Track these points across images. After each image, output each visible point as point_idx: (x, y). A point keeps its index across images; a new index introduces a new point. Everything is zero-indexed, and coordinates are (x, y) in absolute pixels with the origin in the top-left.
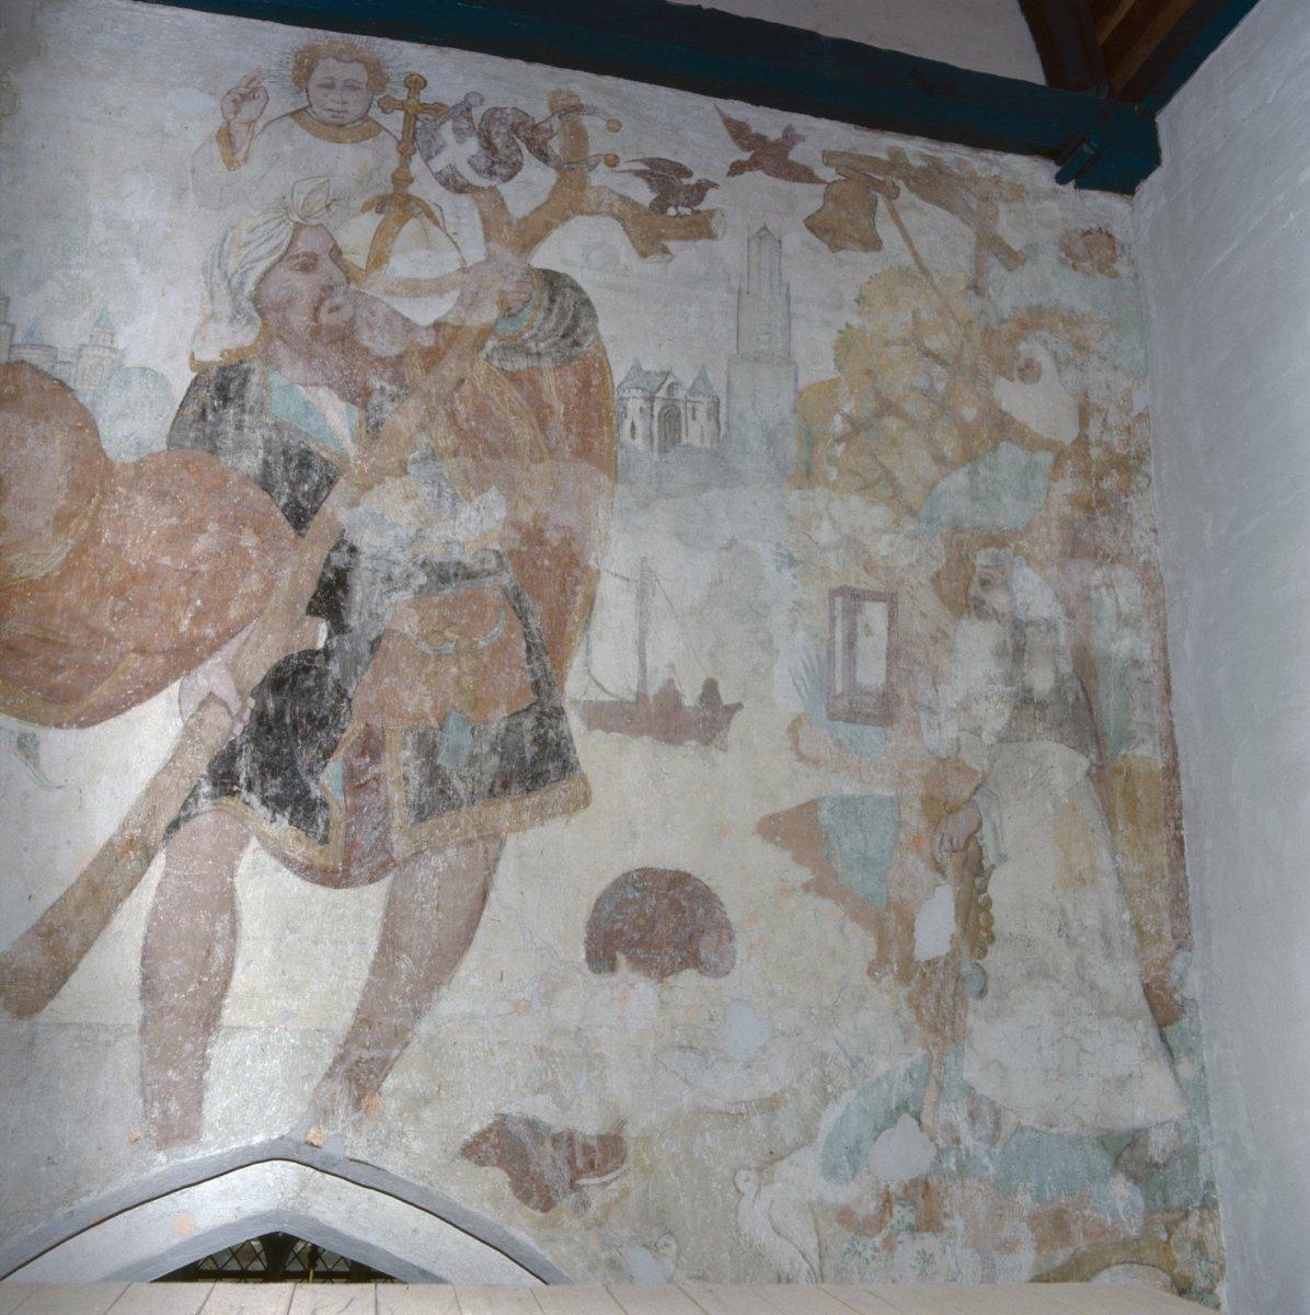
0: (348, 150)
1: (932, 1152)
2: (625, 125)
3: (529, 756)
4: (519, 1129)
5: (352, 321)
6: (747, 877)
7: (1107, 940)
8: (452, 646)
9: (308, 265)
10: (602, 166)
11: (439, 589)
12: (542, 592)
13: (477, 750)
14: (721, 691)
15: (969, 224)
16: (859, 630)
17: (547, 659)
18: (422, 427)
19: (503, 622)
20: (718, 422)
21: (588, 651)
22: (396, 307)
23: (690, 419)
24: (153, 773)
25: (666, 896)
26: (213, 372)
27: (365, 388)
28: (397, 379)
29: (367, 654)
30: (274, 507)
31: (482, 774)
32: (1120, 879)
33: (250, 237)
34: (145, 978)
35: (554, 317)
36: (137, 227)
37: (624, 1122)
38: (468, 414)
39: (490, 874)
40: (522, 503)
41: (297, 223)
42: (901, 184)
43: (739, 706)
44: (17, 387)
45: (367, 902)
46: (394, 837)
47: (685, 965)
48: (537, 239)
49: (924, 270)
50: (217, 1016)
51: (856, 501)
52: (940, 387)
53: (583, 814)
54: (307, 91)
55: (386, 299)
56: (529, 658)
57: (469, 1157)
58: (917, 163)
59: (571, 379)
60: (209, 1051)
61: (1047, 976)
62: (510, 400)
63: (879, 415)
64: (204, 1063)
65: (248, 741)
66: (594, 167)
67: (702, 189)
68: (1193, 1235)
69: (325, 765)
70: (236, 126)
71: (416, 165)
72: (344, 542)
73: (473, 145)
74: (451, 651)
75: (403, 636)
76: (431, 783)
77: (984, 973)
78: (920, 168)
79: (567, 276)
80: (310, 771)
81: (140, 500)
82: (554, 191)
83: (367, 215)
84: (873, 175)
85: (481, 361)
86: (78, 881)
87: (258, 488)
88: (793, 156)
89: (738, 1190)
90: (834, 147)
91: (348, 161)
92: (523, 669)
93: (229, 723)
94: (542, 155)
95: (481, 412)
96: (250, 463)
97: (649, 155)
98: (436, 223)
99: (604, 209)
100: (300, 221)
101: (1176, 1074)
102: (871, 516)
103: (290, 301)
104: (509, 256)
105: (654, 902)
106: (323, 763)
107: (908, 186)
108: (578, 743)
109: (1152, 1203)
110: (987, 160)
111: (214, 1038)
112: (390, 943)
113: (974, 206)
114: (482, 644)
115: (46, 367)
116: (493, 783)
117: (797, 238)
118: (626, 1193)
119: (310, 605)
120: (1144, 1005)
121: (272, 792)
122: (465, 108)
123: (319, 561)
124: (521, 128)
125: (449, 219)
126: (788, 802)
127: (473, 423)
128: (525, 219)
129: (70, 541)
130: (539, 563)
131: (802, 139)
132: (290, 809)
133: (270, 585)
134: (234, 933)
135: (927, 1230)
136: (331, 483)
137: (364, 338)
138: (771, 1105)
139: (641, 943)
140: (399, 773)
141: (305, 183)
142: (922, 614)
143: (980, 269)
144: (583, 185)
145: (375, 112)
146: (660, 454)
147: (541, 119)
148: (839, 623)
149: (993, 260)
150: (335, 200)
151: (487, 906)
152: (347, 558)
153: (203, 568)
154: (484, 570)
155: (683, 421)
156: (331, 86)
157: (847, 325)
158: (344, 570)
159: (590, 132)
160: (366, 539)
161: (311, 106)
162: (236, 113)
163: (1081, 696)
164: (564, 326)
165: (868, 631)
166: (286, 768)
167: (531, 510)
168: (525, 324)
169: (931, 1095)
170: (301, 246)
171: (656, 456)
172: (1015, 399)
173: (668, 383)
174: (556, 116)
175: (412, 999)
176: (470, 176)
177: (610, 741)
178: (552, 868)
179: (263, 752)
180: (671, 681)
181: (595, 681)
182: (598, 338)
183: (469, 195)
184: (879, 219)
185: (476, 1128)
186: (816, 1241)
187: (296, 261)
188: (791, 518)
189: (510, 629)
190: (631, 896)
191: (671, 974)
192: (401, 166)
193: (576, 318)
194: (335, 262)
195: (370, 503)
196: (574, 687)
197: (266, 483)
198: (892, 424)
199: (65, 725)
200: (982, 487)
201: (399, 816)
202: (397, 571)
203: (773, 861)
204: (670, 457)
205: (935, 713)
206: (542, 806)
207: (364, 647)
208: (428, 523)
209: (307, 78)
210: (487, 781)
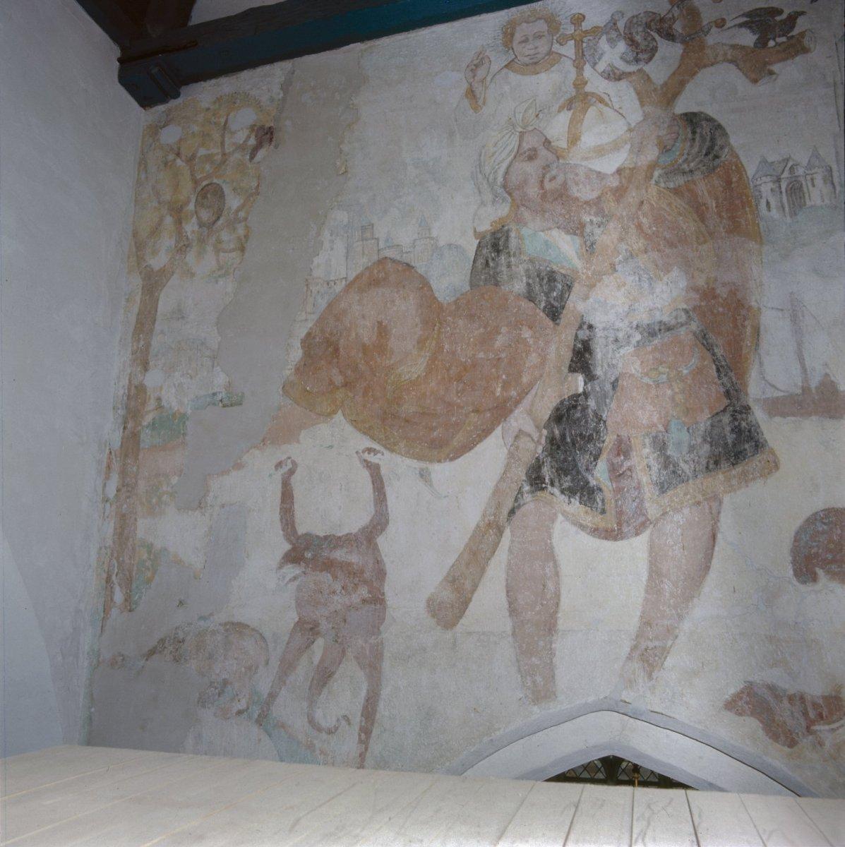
0: (543, 76)
3: (730, 441)
5: (565, 184)
8: (665, 376)
10: (714, 30)
11: (650, 341)
13: (693, 442)
17: (732, 374)
18: (621, 239)
20: (833, 184)
21: (761, 364)
22: (590, 166)
23: (811, 188)
24: (495, 483)
26: (488, 237)
28: (600, 212)
30: (538, 310)
31: (699, 457)
33: (495, 149)
34: (510, 603)
35: (697, 143)
36: (431, 163)
38: (650, 223)
39: (715, 523)
44: (385, 273)
45: (635, 549)
46: (647, 505)
48: (675, 95)
50: (555, 624)
54: (513, 49)
56: (719, 376)
57: (730, 710)
59: (716, 182)
60: (553, 646)
62: (676, 207)
64: (552, 653)
65: (546, 456)
66: (708, 32)
67: (792, 19)
69: (596, 465)
70: (475, 85)
71: (588, 71)
72: (584, 323)
73: (622, 46)
75: (632, 375)
76: (666, 467)
79: (702, 113)
81: (461, 322)
82: (683, 57)
83: (562, 114)
87: (526, 300)
91: (545, 84)
92: (715, 383)
93: (535, 446)
94: (670, 36)
96: (519, 287)
97: (747, 9)
98: (606, 105)
99: (720, 58)
100: (522, 130)
103: (525, 181)
106: (594, 463)
108: (764, 427)
111: (555, 638)
112: (655, 573)
114: (685, 372)
115: (398, 258)
116: (708, 463)
119: (570, 367)
121: (566, 485)
123: (571, 338)
127: (654, 229)
128: (665, 84)
129: (428, 354)
130: (715, 311)
132: (578, 494)
133: (544, 360)
134: (557, 574)
136: (570, 287)
137: (574, 191)
144: (702, 47)
145: (556, 47)
146: (791, 217)
147: (665, 12)
151: (717, 543)
153: (503, 355)
154: (678, 323)
155: (805, 190)
156: (526, 41)
158: (587, 341)
160: (598, 319)
161: (516, 57)
162: (474, 77)
164: (705, 147)
166: (572, 470)
168: (678, 153)
170: (526, 146)
171: (789, 220)
173: (789, 165)
174: (675, 7)
176: (623, 67)
177: (787, 423)
179: (556, 461)
181: (770, 384)
182: (732, 149)
183: (625, 80)
187: (525, 155)
189: (703, 358)
192: (578, 76)
193: (713, 140)
194: (548, 149)
196: (754, 390)
199: (442, 461)
201: (649, 492)
202: (621, 335)
206: (744, 473)
207: (608, 387)
209: (511, 42)
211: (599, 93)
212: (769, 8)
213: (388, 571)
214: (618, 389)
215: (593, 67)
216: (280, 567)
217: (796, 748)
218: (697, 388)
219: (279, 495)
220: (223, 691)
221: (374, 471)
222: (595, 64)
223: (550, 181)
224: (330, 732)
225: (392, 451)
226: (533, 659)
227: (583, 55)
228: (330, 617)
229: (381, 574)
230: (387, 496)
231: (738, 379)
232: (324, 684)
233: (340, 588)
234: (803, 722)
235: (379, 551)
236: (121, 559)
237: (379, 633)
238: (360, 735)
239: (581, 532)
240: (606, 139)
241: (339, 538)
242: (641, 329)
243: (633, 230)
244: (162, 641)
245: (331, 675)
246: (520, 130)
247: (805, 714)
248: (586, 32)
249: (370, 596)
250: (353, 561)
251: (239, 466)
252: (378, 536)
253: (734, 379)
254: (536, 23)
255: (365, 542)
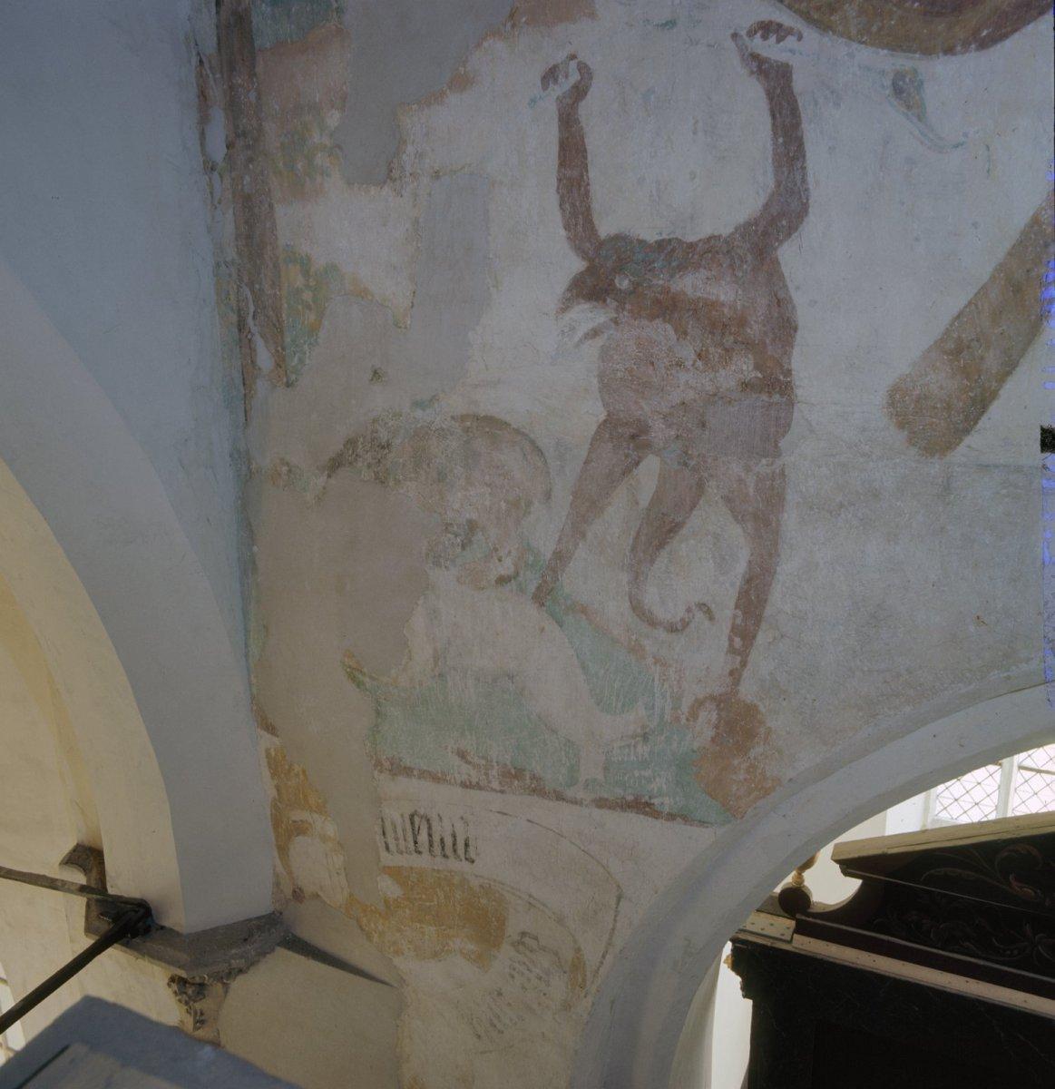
86: (993, 278)
199: (959, 48)
213: (801, 323)
216: (564, 310)
219: (554, 149)
220: (470, 541)
221: (777, 82)
224: (672, 629)
225: (824, 27)
228: (671, 414)
229: (785, 328)
230: (808, 147)
232: (661, 546)
233: (693, 356)
235: (781, 277)
236: (257, 286)
237: (777, 453)
238: (731, 640)
241: (692, 246)
244: (351, 442)
245: (674, 528)
249: (760, 375)
250: (722, 298)
251: (462, 82)
252: (781, 242)
255: (749, 257)
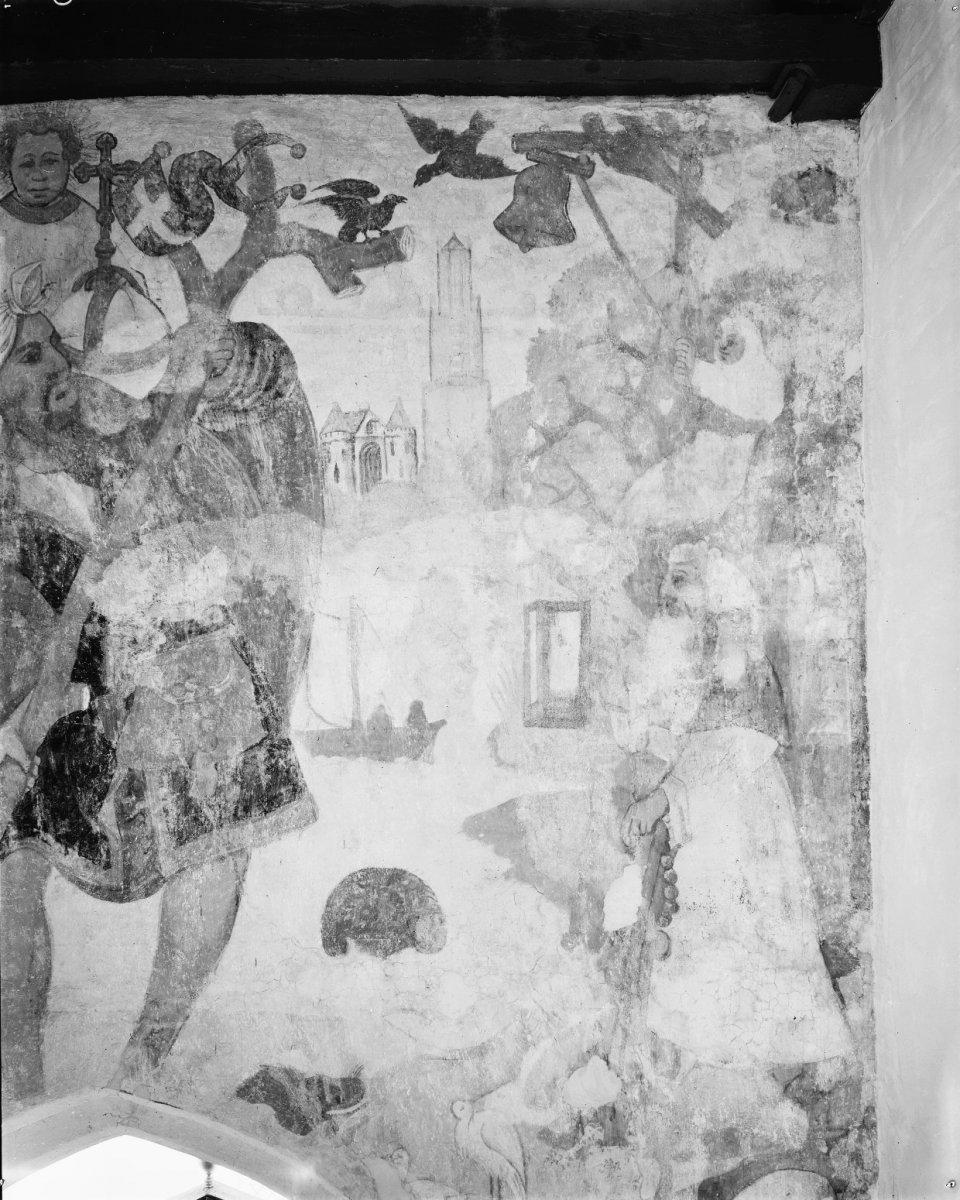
0: (53, 229)
1: (618, 1086)
2: (309, 148)
3: (264, 783)
4: (280, 1077)
5: (76, 407)
6: (454, 872)
7: (787, 906)
8: (192, 695)
9: (33, 358)
11: (177, 647)
12: (265, 635)
14: (426, 710)
15: (669, 191)
16: (554, 640)
17: (272, 698)
18: (149, 499)
19: (233, 670)
20: (415, 454)
22: (116, 385)
25: (385, 890)
27: (96, 468)
28: (123, 455)
29: (124, 710)
31: (226, 801)
32: (804, 850)
35: (256, 371)
37: (361, 1068)
38: (187, 479)
39: (240, 883)
40: (241, 559)
41: (18, 315)
42: (596, 158)
43: (443, 722)
45: (145, 911)
46: (161, 858)
47: (404, 945)
48: (234, 292)
49: (620, 255)
50: (44, 1005)
51: (550, 515)
52: (636, 382)
53: (312, 828)
55: (105, 378)
56: (257, 699)
58: (614, 128)
59: (277, 432)
60: (41, 1030)
61: (726, 937)
63: (572, 422)
64: (39, 1039)
65: (40, 792)
66: (282, 202)
67: (389, 205)
68: (852, 1148)
71: (116, 234)
72: (95, 614)
73: (165, 202)
74: (192, 700)
75: (151, 691)
76: (186, 813)
77: (668, 938)
78: (618, 133)
80: (90, 812)
82: (247, 235)
83: (78, 295)
84: (566, 153)
85: (194, 425)
88: (481, 149)
89: (455, 1116)
90: (524, 129)
91: (56, 239)
94: (232, 199)
95: (199, 476)
98: (140, 292)
99: (295, 246)
101: (845, 1017)
102: (563, 528)
103: (23, 395)
104: (208, 314)
105: (376, 896)
106: (99, 804)
107: (604, 158)
109: (816, 1123)
110: (693, 108)
111: (44, 1021)
112: (167, 944)
113: (676, 168)
116: (236, 809)
117: (487, 242)
118: (366, 1120)
119: (74, 673)
120: (820, 959)
121: (63, 831)
122: (155, 160)
123: (76, 633)
124: (209, 173)
125: (152, 285)
126: (490, 802)
127: (192, 488)
128: (221, 272)
131: (490, 125)
133: (40, 661)
134: (48, 943)
135: (614, 1144)
136: (77, 562)
137: (91, 420)
138: (481, 1051)
139: (367, 930)
140: (159, 808)
141: (21, 271)
142: (615, 619)
143: (681, 242)
144: (273, 225)
148: (533, 636)
149: (695, 229)
150: (48, 285)
152: (98, 628)
154: (213, 625)
156: (29, 165)
157: (540, 331)
159: (277, 164)
160: (112, 610)
161: (16, 189)
163: (772, 680)
164: (266, 378)
165: (562, 641)
167: (250, 564)
168: (230, 382)
169: (618, 1040)
170: (26, 339)
171: (359, 497)
172: (713, 381)
174: (241, 152)
175: (187, 983)
176: (166, 235)
177: (331, 764)
178: (291, 872)
180: (382, 706)
183: (167, 256)
184: (572, 204)
185: (246, 1076)
186: (520, 1153)
188: (486, 540)
189: (240, 675)
190: (356, 892)
191: (393, 952)
192: (102, 238)
193: (276, 369)
195: (109, 575)
196: (300, 722)
197: (24, 569)
198: (586, 429)
200: (677, 482)
201: (164, 842)
202: (140, 635)
203: (480, 853)
204: (373, 494)
205: (626, 712)
206: (278, 824)
207: (121, 704)
208: (160, 587)
210: (231, 807)
211: (129, 270)
212: (362, 182)
214: (134, 708)
215: (124, 228)
217: (308, 1136)
218: (230, 714)
222: (127, 223)
223: (58, 398)
226: (17, 1046)
227: (111, 205)
231: (280, 704)
234: (319, 1107)
239: (79, 891)
240: (136, 346)
242: (166, 629)
243: (165, 486)
246: (18, 311)
247: (322, 1098)
248: (117, 168)
253: (275, 705)
254: (46, 137)
